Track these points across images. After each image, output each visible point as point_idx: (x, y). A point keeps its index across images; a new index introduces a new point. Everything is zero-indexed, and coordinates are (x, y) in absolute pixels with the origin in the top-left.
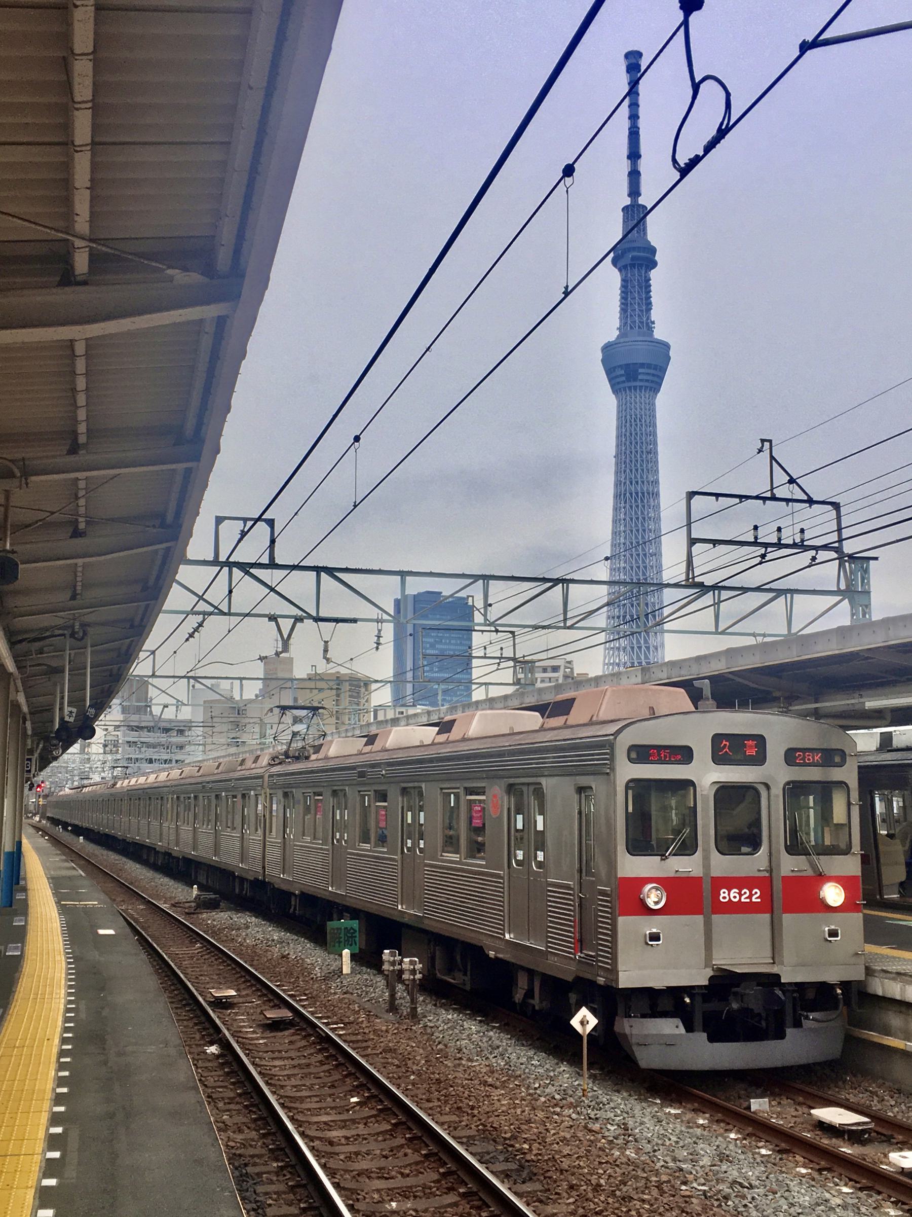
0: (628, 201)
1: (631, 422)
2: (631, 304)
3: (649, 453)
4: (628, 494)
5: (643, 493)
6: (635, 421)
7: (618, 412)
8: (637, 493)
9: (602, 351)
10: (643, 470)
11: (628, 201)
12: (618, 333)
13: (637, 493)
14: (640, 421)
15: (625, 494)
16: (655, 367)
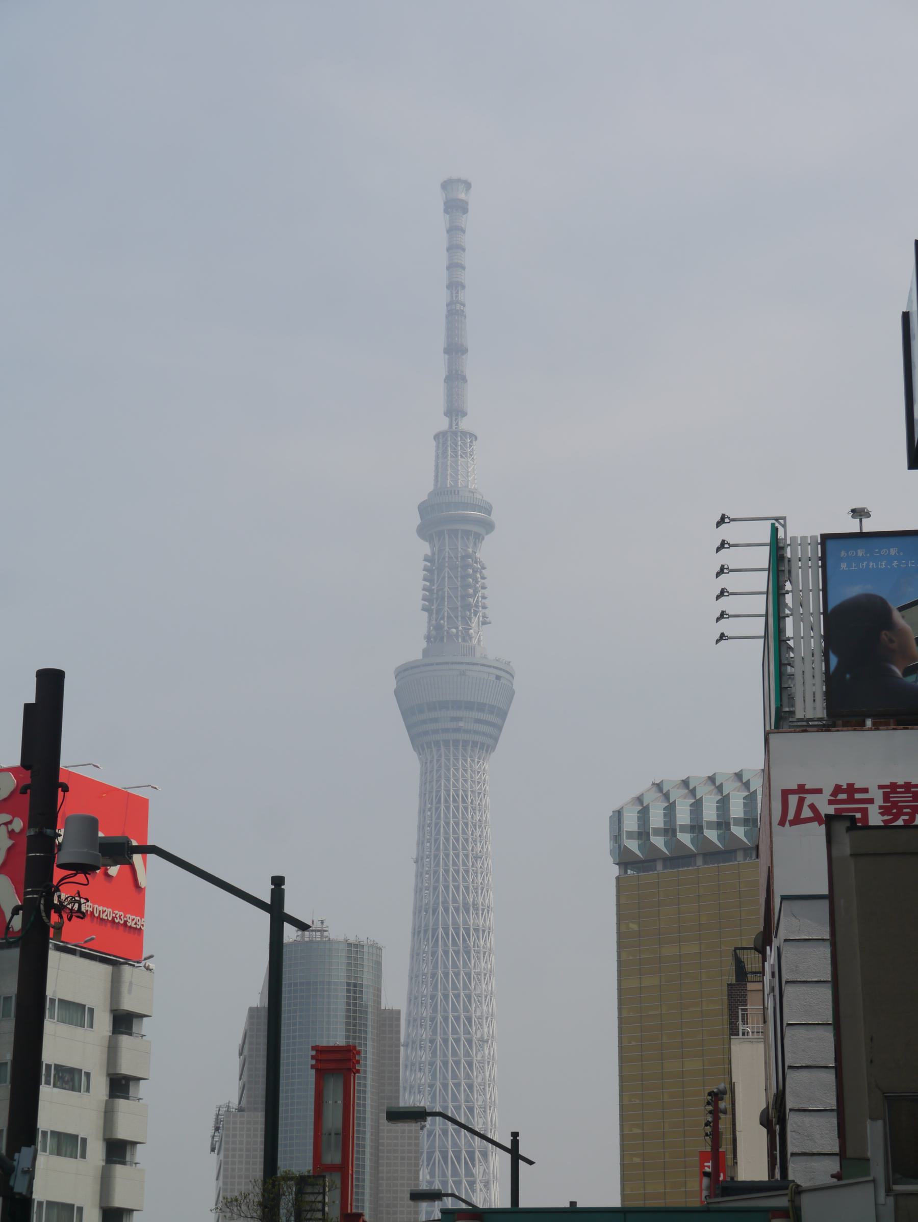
0: (443, 424)
1: (446, 801)
2: (449, 597)
3: (476, 858)
4: (441, 930)
5: (467, 930)
6: (455, 801)
7: (423, 784)
8: (457, 930)
9: (396, 677)
10: (467, 888)
11: (443, 424)
12: (424, 645)
13: (457, 930)
14: (464, 801)
15: (435, 930)
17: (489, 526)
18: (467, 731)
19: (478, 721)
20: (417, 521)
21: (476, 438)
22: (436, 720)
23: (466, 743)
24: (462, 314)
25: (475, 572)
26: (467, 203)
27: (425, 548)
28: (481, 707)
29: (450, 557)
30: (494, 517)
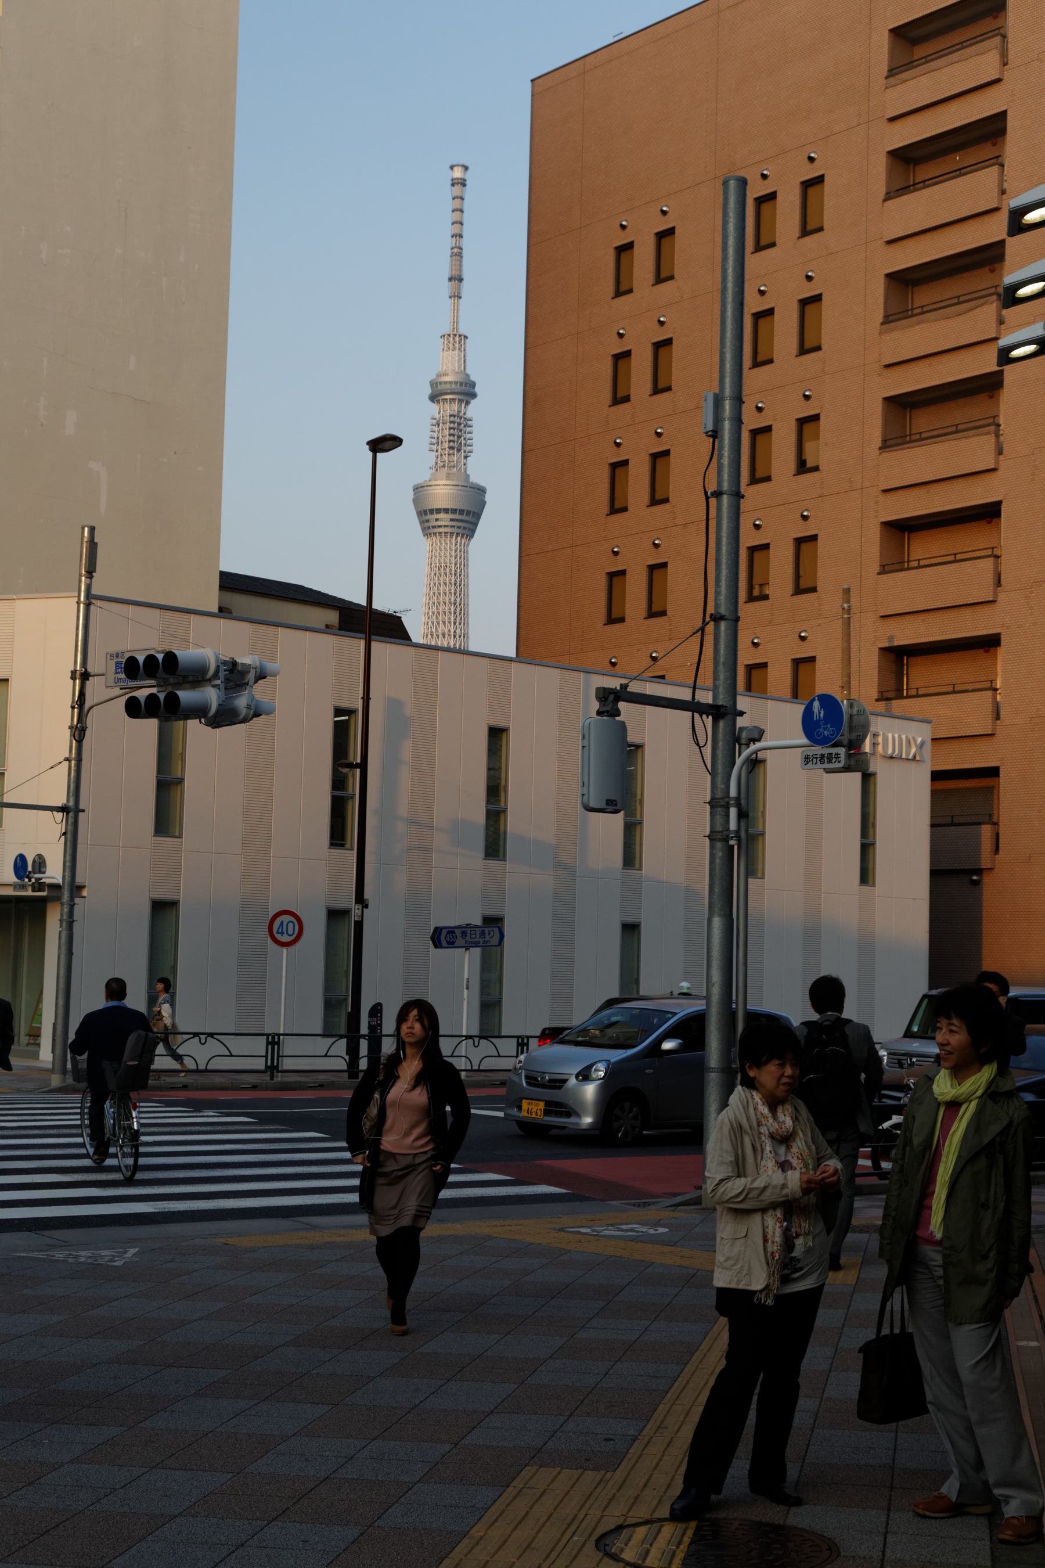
0: (447, 330)
2: (442, 442)
9: (414, 490)
16: (468, 513)
17: (474, 396)
18: (446, 526)
19: (452, 520)
20: (429, 391)
21: (467, 338)
22: (428, 521)
23: (445, 533)
24: (460, 255)
25: (459, 424)
26: (465, 180)
27: (434, 409)
28: (454, 511)
29: (443, 417)
30: (477, 389)
